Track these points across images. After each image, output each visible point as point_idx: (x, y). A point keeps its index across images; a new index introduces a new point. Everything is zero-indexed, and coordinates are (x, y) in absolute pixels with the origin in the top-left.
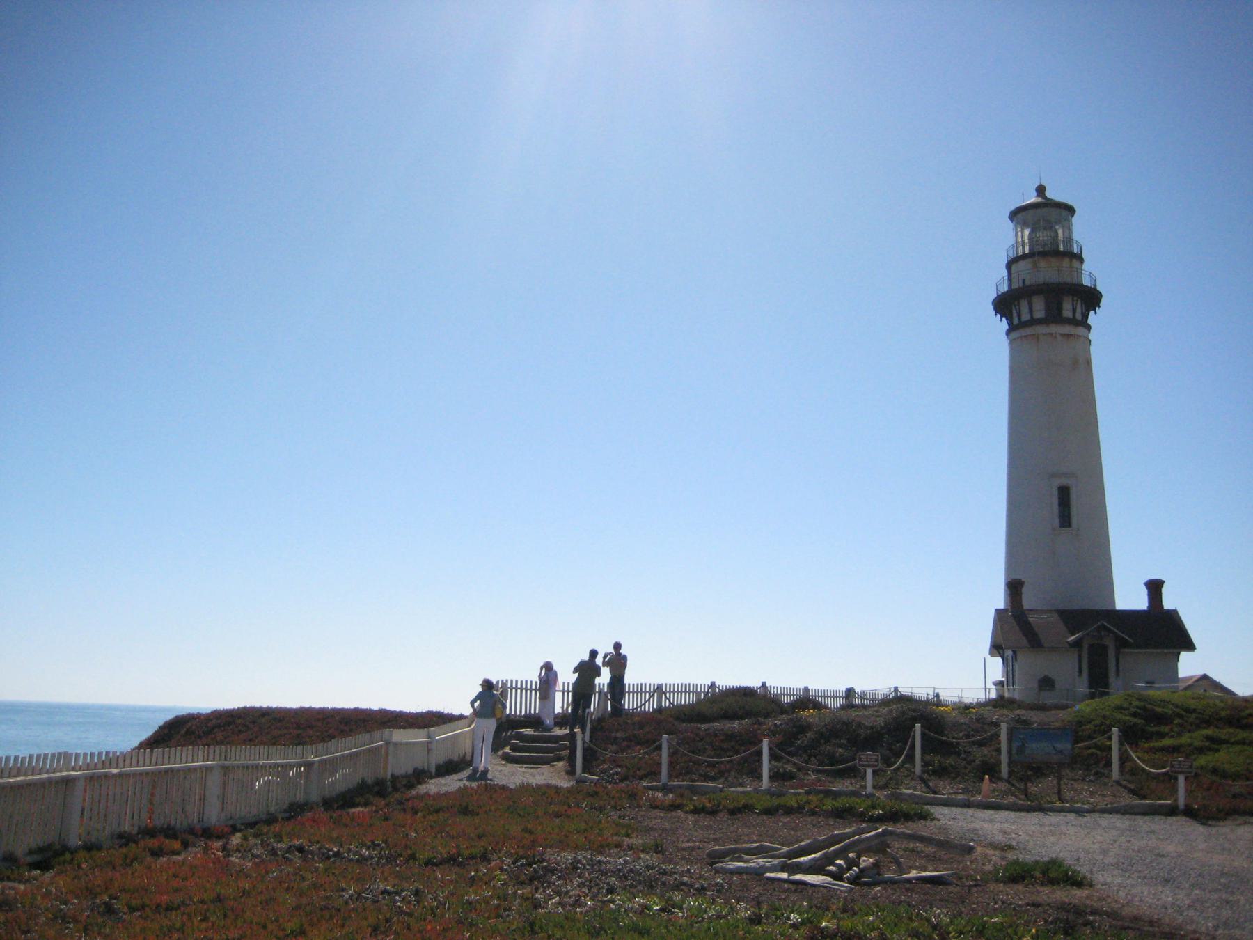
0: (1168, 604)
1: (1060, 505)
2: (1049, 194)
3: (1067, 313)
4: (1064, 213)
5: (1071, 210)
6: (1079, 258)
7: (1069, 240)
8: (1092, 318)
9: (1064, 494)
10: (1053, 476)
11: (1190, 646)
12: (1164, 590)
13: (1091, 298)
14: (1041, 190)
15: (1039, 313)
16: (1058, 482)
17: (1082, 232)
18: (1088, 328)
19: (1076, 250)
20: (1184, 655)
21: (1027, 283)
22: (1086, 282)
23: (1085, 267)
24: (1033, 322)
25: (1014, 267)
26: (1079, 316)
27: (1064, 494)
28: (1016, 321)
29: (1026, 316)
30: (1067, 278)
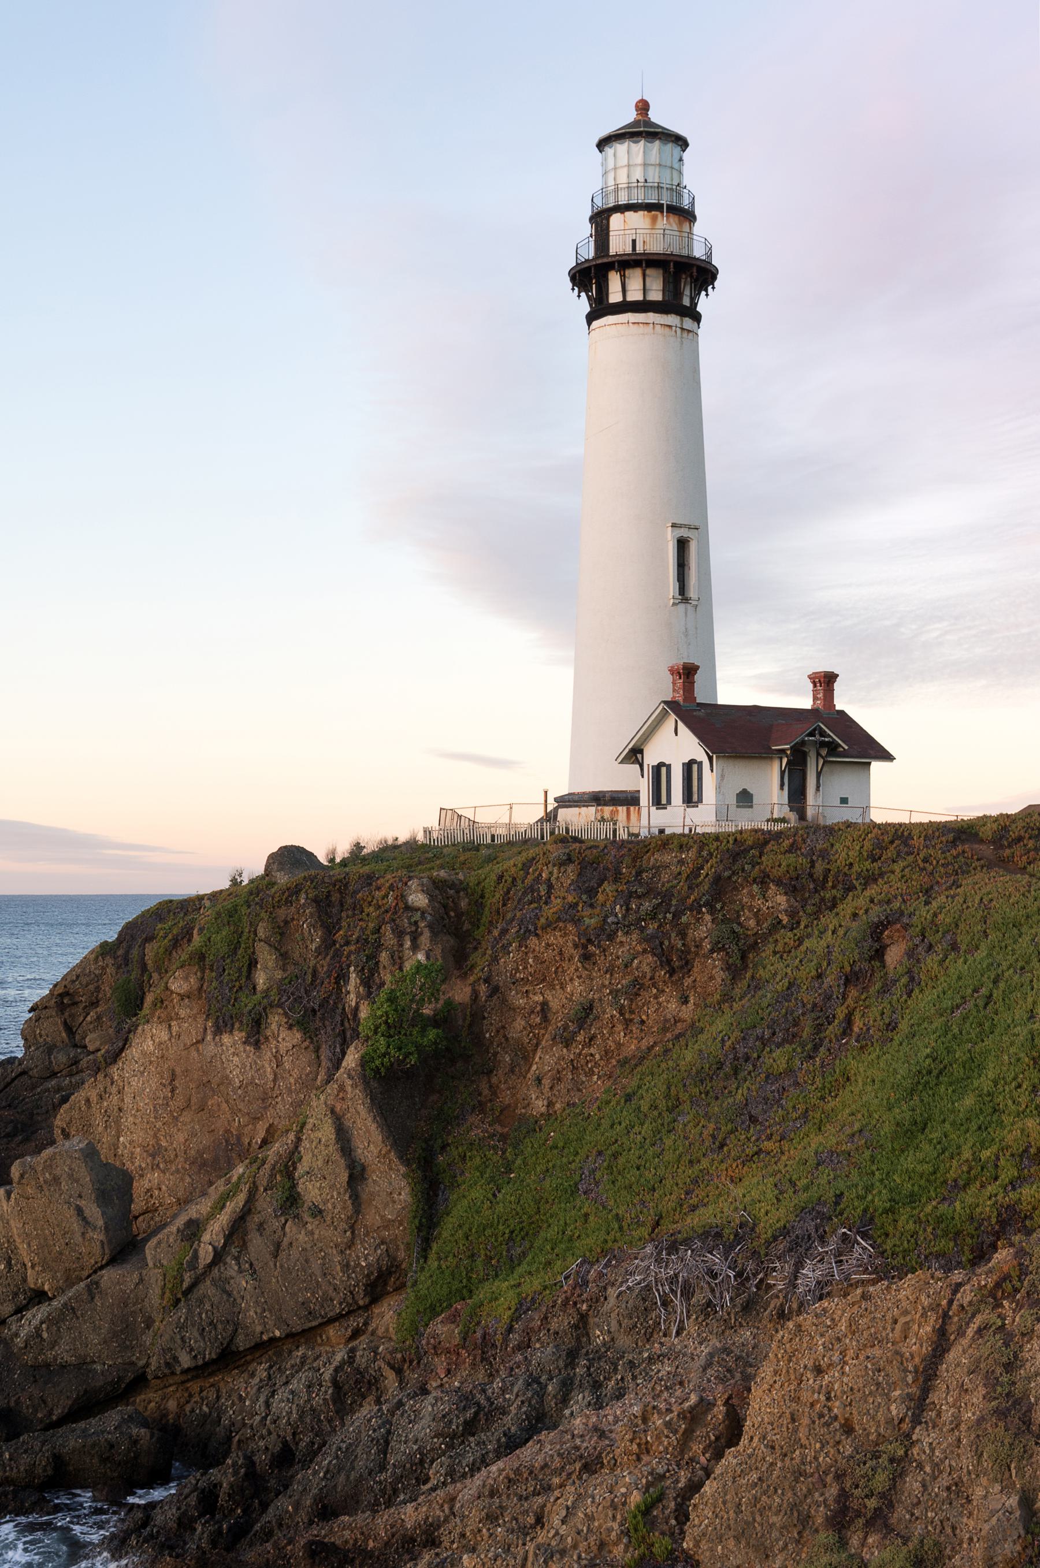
2: (654, 116)
3: (686, 302)
5: (681, 142)
7: (678, 189)
8: (704, 304)
9: (682, 545)
10: (674, 526)
11: (887, 756)
13: (703, 275)
17: (699, 178)
20: (877, 767)
21: (639, 249)
22: (699, 252)
23: (698, 228)
26: (686, 302)
28: (615, 296)
29: (635, 295)
30: (676, 249)
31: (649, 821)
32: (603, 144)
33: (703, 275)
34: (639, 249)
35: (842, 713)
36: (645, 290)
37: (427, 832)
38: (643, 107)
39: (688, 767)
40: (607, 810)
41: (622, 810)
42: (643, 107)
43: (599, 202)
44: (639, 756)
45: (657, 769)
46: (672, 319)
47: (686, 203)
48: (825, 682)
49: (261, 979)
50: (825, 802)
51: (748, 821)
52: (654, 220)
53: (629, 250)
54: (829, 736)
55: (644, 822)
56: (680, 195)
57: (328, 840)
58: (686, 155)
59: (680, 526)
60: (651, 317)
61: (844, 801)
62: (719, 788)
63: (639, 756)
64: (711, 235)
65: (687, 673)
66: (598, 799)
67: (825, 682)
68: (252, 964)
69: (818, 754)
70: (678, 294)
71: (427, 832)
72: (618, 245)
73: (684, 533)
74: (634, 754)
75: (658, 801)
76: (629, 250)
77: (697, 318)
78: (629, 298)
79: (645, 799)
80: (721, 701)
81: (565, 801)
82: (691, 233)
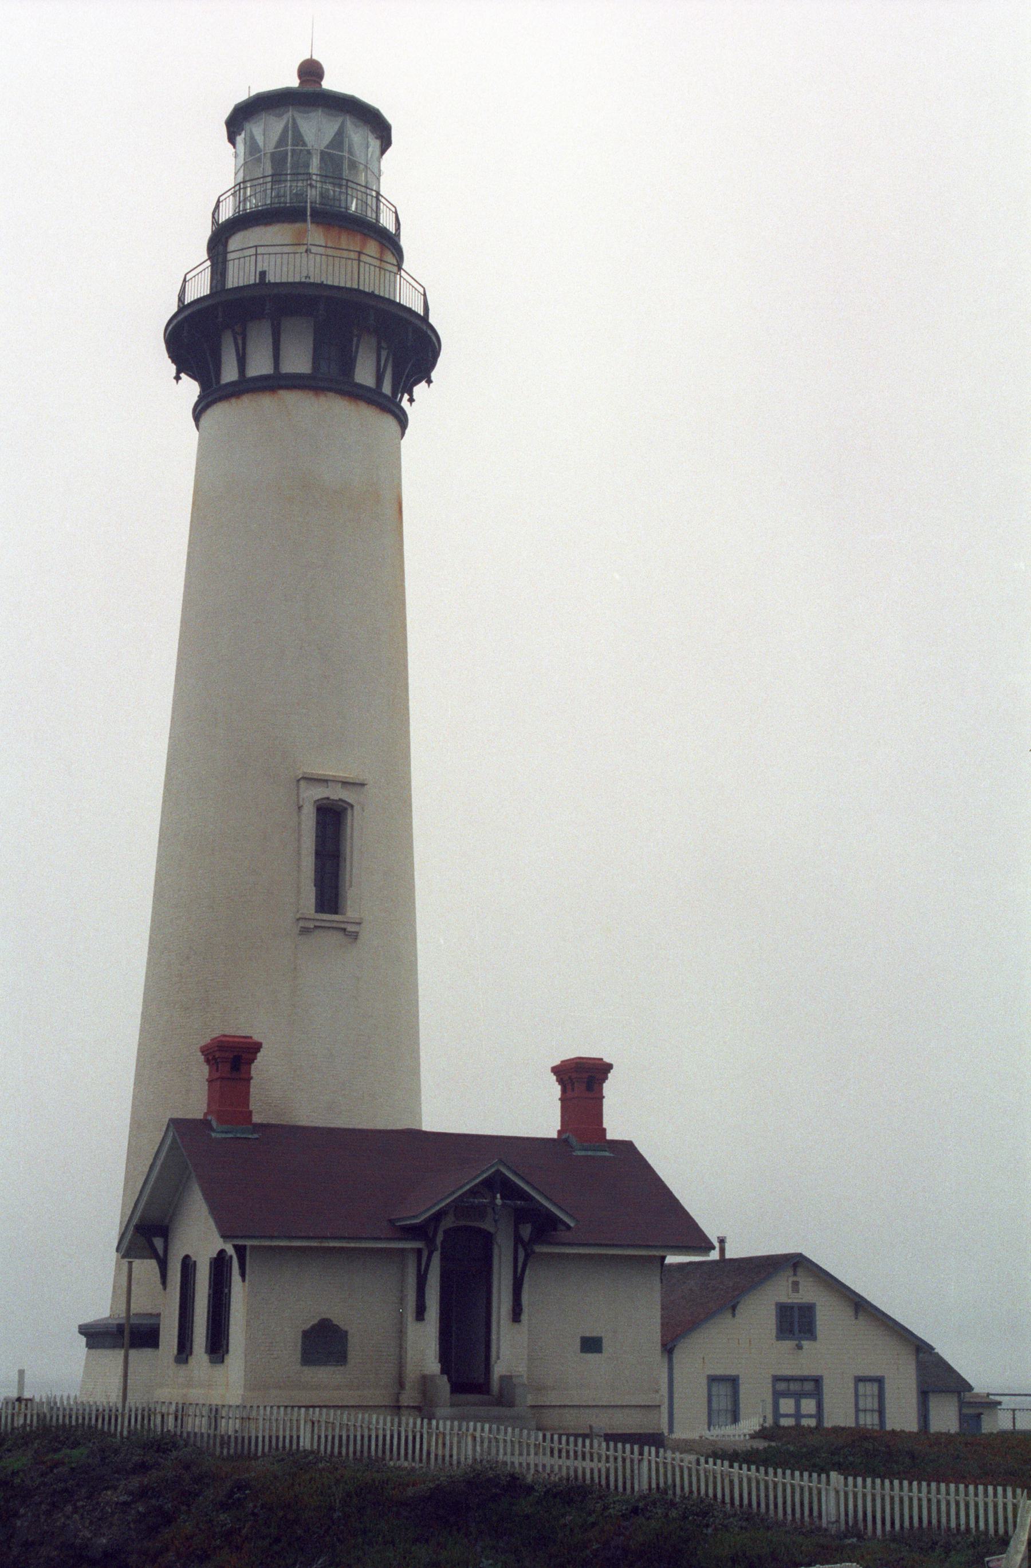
0: (615, 1127)
1: (318, 854)
3: (364, 375)
4: (358, 136)
12: (610, 1088)
14: (311, 71)
15: (298, 361)
16: (319, 793)
18: (403, 421)
19: (387, 221)
25: (235, 243)
27: (332, 818)
28: (229, 374)
29: (260, 365)
35: (627, 1148)
39: (220, 1265)
44: (158, 1243)
48: (582, 1081)
54: (528, 1198)
59: (324, 781)
63: (158, 1243)
64: (430, 276)
65: (231, 1061)
67: (582, 1081)
69: (518, 1240)
70: (348, 366)
73: (336, 793)
78: (252, 372)
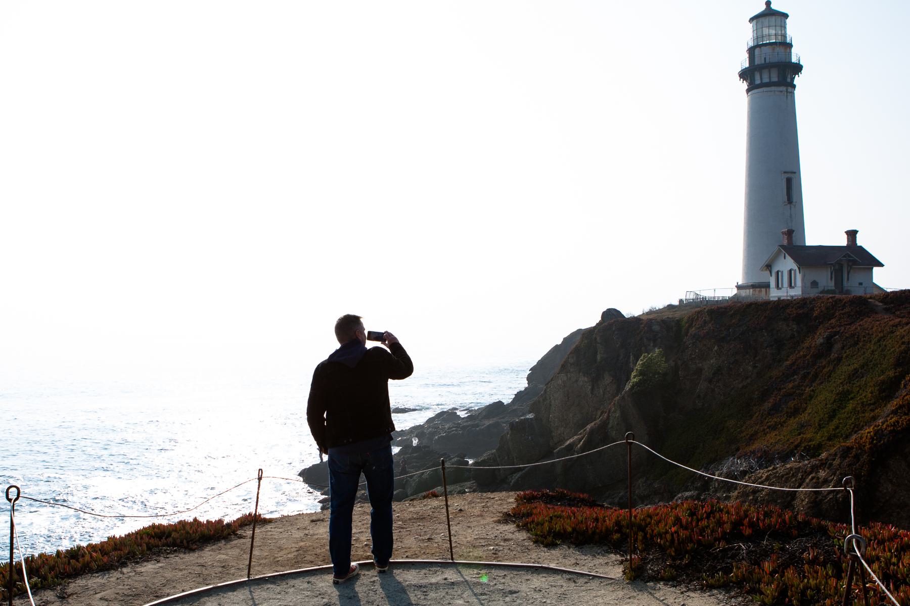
2: (773, 6)
3: (789, 80)
5: (786, 16)
6: (790, 46)
7: (785, 36)
8: (797, 80)
9: (789, 182)
10: (785, 172)
13: (798, 68)
15: (775, 79)
17: (793, 31)
21: (767, 61)
23: (793, 50)
24: (770, 84)
25: (757, 51)
27: (789, 182)
29: (766, 80)
31: (775, 294)
32: (751, 20)
33: (797, 68)
34: (767, 61)
36: (770, 77)
37: (681, 301)
38: (768, 4)
40: (758, 290)
41: (764, 290)
42: (768, 4)
43: (751, 44)
45: (778, 272)
46: (783, 88)
47: (788, 41)
49: (599, 357)
50: (853, 285)
51: (813, 293)
52: (774, 49)
53: (763, 62)
55: (772, 295)
56: (785, 37)
57: (632, 308)
58: (788, 21)
60: (773, 88)
61: (861, 284)
62: (803, 280)
66: (753, 286)
68: (596, 353)
70: (785, 78)
71: (681, 301)
72: (757, 62)
74: (769, 267)
75: (777, 287)
76: (763, 62)
77: (794, 87)
79: (773, 284)
80: (807, 244)
81: (739, 287)
82: (790, 52)
